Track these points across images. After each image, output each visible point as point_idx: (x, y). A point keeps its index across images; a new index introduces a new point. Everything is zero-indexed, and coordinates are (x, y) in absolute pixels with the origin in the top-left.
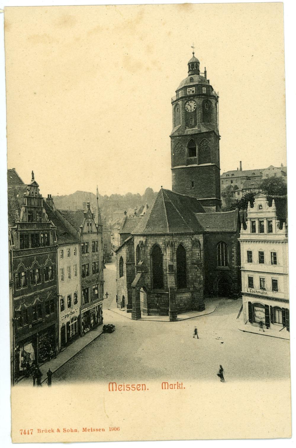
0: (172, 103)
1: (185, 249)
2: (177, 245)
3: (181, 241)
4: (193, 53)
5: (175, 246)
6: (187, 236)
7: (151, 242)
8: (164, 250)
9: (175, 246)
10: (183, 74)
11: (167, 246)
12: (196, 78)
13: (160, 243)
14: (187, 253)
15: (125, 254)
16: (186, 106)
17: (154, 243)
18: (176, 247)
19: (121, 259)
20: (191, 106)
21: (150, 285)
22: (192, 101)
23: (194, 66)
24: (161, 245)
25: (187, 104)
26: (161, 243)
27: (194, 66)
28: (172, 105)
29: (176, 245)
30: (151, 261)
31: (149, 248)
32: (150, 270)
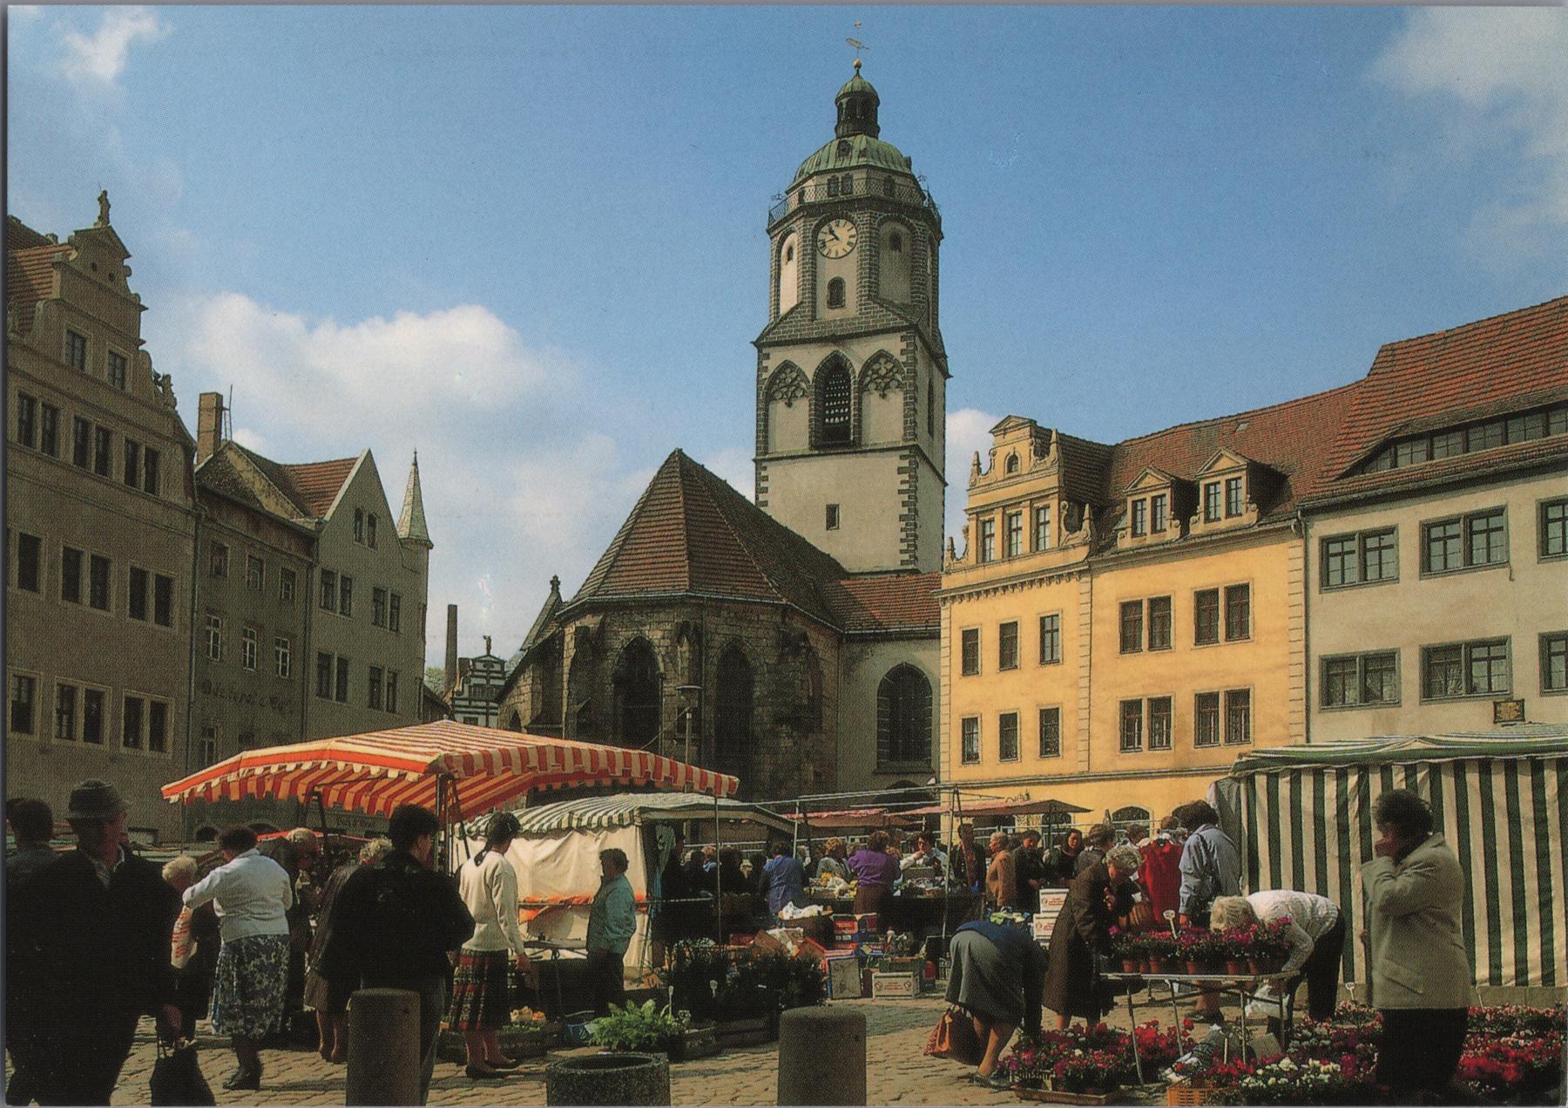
0: (768, 232)
2: (718, 640)
4: (858, 66)
7: (621, 637)
11: (679, 642)
12: (859, 142)
13: (656, 635)
14: (757, 678)
15: (527, 697)
16: (821, 236)
18: (715, 655)
22: (842, 222)
25: (825, 229)
26: (659, 634)
27: (859, 110)
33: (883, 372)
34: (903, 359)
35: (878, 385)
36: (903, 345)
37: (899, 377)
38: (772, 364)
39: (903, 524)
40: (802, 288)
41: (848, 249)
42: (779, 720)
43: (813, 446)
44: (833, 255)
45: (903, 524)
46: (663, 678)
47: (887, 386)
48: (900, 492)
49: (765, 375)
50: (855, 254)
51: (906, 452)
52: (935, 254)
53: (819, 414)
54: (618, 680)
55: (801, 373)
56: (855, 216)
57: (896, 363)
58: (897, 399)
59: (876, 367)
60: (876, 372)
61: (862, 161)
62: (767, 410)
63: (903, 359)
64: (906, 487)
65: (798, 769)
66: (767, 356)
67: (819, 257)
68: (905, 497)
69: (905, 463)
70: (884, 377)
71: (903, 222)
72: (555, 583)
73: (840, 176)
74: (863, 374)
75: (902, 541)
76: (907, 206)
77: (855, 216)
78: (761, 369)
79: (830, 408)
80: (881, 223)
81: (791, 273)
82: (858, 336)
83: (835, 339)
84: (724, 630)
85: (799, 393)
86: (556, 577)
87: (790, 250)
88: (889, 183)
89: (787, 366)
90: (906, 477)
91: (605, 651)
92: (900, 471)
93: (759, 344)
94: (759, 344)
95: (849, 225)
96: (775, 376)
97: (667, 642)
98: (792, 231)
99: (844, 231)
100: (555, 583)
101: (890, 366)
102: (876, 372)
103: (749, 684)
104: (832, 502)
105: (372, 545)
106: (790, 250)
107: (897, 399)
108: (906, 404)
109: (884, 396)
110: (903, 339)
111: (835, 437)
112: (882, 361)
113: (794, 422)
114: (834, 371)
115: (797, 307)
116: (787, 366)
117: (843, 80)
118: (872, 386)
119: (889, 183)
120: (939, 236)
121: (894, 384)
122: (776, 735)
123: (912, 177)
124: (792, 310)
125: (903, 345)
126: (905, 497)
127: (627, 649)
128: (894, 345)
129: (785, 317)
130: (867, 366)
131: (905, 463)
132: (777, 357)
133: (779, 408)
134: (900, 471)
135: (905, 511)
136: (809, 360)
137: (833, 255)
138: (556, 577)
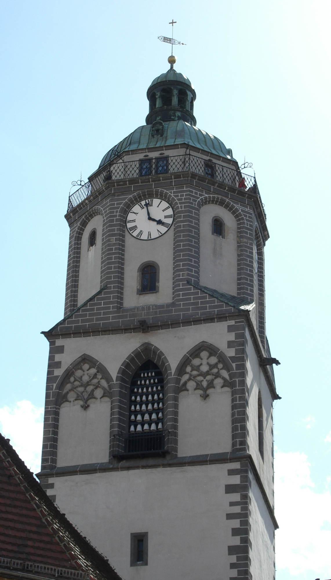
20: (150, 219)
23: (171, 97)
28: (70, 225)
33: (205, 368)
34: (231, 353)
35: (199, 386)
36: (232, 337)
37: (225, 374)
38: (67, 360)
39: (233, 559)
40: (105, 272)
44: (144, 236)
45: (233, 559)
47: (211, 385)
48: (230, 516)
49: (59, 372)
51: (236, 465)
52: (260, 254)
55: (102, 370)
56: (171, 193)
57: (222, 358)
58: (221, 399)
59: (196, 362)
60: (197, 368)
61: (179, 141)
62: (57, 414)
63: (231, 353)
64: (237, 509)
67: (129, 241)
68: (236, 523)
69: (236, 480)
70: (204, 375)
71: (230, 209)
74: (181, 370)
76: (232, 189)
77: (171, 193)
78: (53, 365)
79: (136, 413)
80: (206, 202)
83: (144, 327)
85: (98, 393)
88: (209, 166)
89: (85, 359)
90: (236, 497)
92: (230, 489)
95: (165, 204)
96: (69, 374)
99: (160, 209)
101: (214, 360)
102: (197, 368)
104: (139, 529)
107: (221, 399)
108: (233, 407)
109: (205, 397)
110: (230, 329)
112: (204, 354)
113: (94, 427)
114: (146, 368)
115: (99, 293)
118: (191, 385)
119: (209, 166)
120: (262, 234)
121: (218, 382)
123: (235, 163)
124: (91, 299)
125: (232, 337)
126: (236, 523)
128: (219, 335)
131: (236, 480)
132: (74, 348)
133: (70, 411)
134: (230, 489)
135: (236, 541)
136: (114, 352)
137: (144, 236)
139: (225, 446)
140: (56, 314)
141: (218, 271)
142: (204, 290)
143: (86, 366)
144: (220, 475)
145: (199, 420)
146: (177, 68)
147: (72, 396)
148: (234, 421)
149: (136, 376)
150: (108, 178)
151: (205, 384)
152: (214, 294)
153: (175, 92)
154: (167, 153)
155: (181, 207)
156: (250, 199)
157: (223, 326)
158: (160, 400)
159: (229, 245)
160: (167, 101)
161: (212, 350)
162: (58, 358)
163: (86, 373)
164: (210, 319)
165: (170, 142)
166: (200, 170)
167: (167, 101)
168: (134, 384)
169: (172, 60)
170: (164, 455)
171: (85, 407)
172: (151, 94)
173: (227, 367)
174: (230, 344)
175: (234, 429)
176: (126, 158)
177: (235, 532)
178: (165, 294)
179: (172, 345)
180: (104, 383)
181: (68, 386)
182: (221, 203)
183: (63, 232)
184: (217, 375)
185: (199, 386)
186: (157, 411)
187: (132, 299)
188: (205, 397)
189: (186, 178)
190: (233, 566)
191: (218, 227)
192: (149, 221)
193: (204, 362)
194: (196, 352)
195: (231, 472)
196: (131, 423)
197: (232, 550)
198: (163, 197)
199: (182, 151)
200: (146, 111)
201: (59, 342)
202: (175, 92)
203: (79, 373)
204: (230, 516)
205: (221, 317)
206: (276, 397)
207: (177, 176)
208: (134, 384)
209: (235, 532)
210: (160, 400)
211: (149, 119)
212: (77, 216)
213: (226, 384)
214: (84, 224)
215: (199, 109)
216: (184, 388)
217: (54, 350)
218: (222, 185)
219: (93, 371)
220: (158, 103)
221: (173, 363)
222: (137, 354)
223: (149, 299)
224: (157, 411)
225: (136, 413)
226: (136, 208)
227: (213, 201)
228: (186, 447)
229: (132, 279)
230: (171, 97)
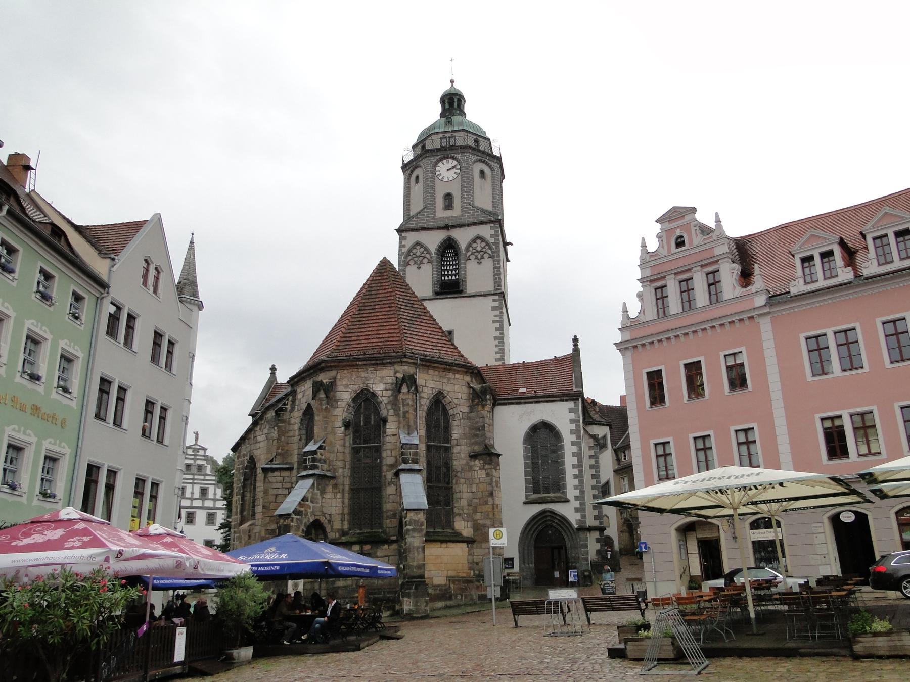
1: (451, 412)
3: (439, 386)
4: (452, 82)
5: (421, 397)
6: (457, 376)
8: (389, 407)
9: (421, 397)
10: (433, 113)
16: (438, 169)
17: (358, 387)
19: (252, 461)
21: (338, 518)
23: (452, 103)
24: (379, 393)
29: (425, 395)
30: (347, 444)
31: (342, 404)
32: (341, 471)
33: (479, 249)
36: (493, 232)
37: (489, 251)
38: (409, 243)
41: (455, 176)
42: (474, 456)
43: (437, 293)
45: (497, 343)
46: (385, 421)
47: (482, 257)
48: (494, 322)
49: (405, 250)
50: (459, 179)
51: (497, 297)
53: (441, 271)
54: (347, 425)
55: (426, 249)
56: (458, 156)
57: (487, 244)
58: (488, 263)
59: (474, 245)
63: (492, 240)
64: (498, 318)
65: (491, 494)
66: (405, 238)
68: (497, 325)
69: (497, 304)
72: (273, 369)
73: (447, 135)
74: (467, 249)
75: (496, 353)
77: (458, 156)
78: (401, 246)
79: (444, 270)
81: (418, 190)
82: (463, 226)
83: (447, 227)
84: (431, 384)
85: (425, 261)
86: (273, 365)
87: (417, 177)
88: (476, 141)
90: (497, 312)
91: (337, 401)
92: (494, 308)
93: (399, 231)
94: (399, 231)
96: (410, 251)
97: (389, 393)
98: (419, 166)
100: (273, 369)
101: (483, 244)
103: (447, 429)
105: (155, 292)
106: (417, 177)
107: (488, 263)
109: (480, 263)
110: (492, 228)
111: (450, 288)
112: (478, 241)
116: (418, 244)
117: (446, 87)
118: (472, 257)
121: (486, 256)
122: (471, 469)
125: (493, 232)
126: (497, 325)
127: (354, 400)
128: (486, 231)
129: (413, 217)
130: (469, 245)
131: (497, 304)
132: (412, 238)
134: (494, 308)
135: (498, 334)
136: (433, 240)
138: (273, 365)
139: (490, 288)
140: (399, 220)
141: (483, 200)
142: (477, 208)
143: (418, 247)
144: (489, 302)
145: (476, 275)
146: (456, 86)
147: (412, 263)
148: (495, 275)
149: (444, 252)
150: (423, 147)
151: (479, 257)
152: (482, 210)
153: (456, 100)
154: (454, 134)
155: (464, 164)
156: (499, 159)
157: (488, 227)
158: (456, 264)
159: (488, 184)
160: (451, 104)
161: (483, 239)
162: (404, 242)
163: (418, 251)
164: (481, 223)
165: (456, 128)
166: (472, 144)
167: (451, 104)
168: (443, 256)
169: (452, 82)
170: (461, 292)
171: (419, 268)
172: (442, 100)
173: (490, 248)
174: (492, 236)
175: (495, 279)
176: (433, 137)
177: (497, 329)
178: (456, 211)
179: (462, 237)
180: (428, 256)
181: (410, 258)
182: (484, 162)
183: (400, 177)
184: (485, 252)
185: (476, 258)
186: (455, 269)
187: (441, 213)
188: (480, 263)
189: (465, 148)
190: (496, 346)
191: (482, 172)
192: (446, 170)
193: (479, 245)
194: (474, 241)
195: (494, 300)
196: (442, 275)
197: (496, 338)
198: (454, 158)
199: (463, 134)
200: (440, 110)
201: (404, 234)
202: (456, 100)
203: (414, 251)
204: (494, 322)
205: (487, 223)
206: (508, 260)
207: (461, 147)
208: (443, 256)
209: (497, 329)
210: (456, 264)
211: (442, 115)
212: (408, 168)
213: (490, 257)
214: (412, 172)
215: (467, 108)
216: (468, 259)
217: (402, 239)
218: (484, 152)
219: (422, 250)
220: (447, 106)
221: (463, 245)
222: (445, 241)
223: (449, 213)
224: (455, 269)
225: (444, 270)
226: (440, 164)
227: (480, 161)
228: (471, 287)
229: (440, 202)
230: (452, 103)
